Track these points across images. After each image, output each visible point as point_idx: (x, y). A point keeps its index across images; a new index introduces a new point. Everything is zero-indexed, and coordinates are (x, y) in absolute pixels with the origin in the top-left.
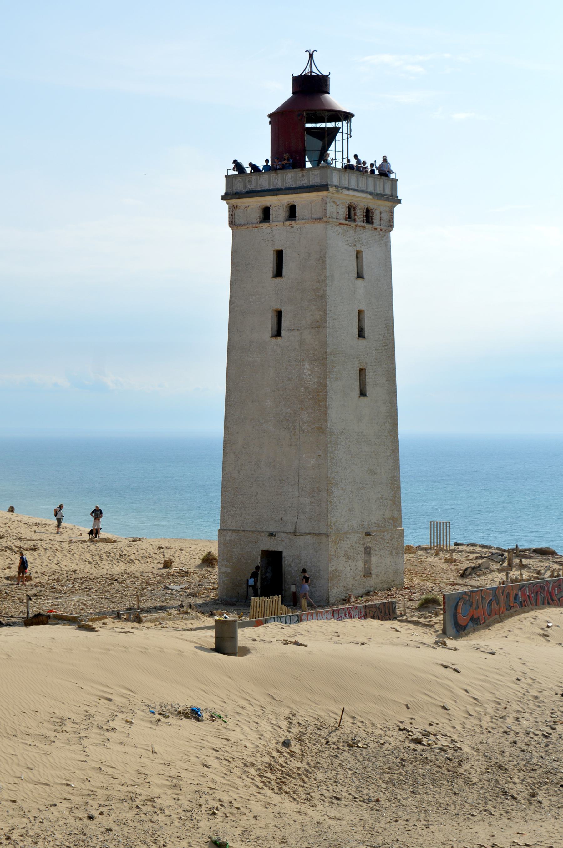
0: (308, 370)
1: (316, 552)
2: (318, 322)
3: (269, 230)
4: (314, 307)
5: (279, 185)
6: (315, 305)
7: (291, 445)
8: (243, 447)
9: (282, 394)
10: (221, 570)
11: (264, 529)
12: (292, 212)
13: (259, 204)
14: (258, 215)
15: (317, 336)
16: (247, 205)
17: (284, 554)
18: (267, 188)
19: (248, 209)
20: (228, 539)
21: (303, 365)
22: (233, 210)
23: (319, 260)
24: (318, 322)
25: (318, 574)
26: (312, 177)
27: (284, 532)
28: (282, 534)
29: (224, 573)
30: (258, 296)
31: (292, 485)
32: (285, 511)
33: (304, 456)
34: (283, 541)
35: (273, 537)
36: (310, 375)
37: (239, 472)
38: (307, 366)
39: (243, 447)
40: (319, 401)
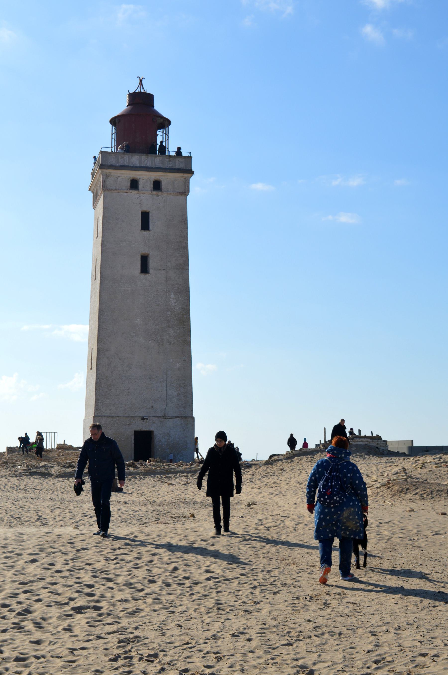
0: (173, 298)
1: (184, 430)
3: (137, 195)
4: (177, 255)
5: (149, 165)
6: (178, 253)
8: (116, 354)
11: (136, 415)
12: (157, 185)
13: (130, 176)
15: (181, 275)
16: (119, 175)
17: (155, 433)
18: (138, 165)
19: (119, 179)
22: (105, 177)
23: (181, 222)
26: (177, 163)
28: (154, 418)
30: (128, 243)
33: (171, 360)
35: (145, 421)
37: (112, 372)
38: (172, 296)
39: (116, 354)
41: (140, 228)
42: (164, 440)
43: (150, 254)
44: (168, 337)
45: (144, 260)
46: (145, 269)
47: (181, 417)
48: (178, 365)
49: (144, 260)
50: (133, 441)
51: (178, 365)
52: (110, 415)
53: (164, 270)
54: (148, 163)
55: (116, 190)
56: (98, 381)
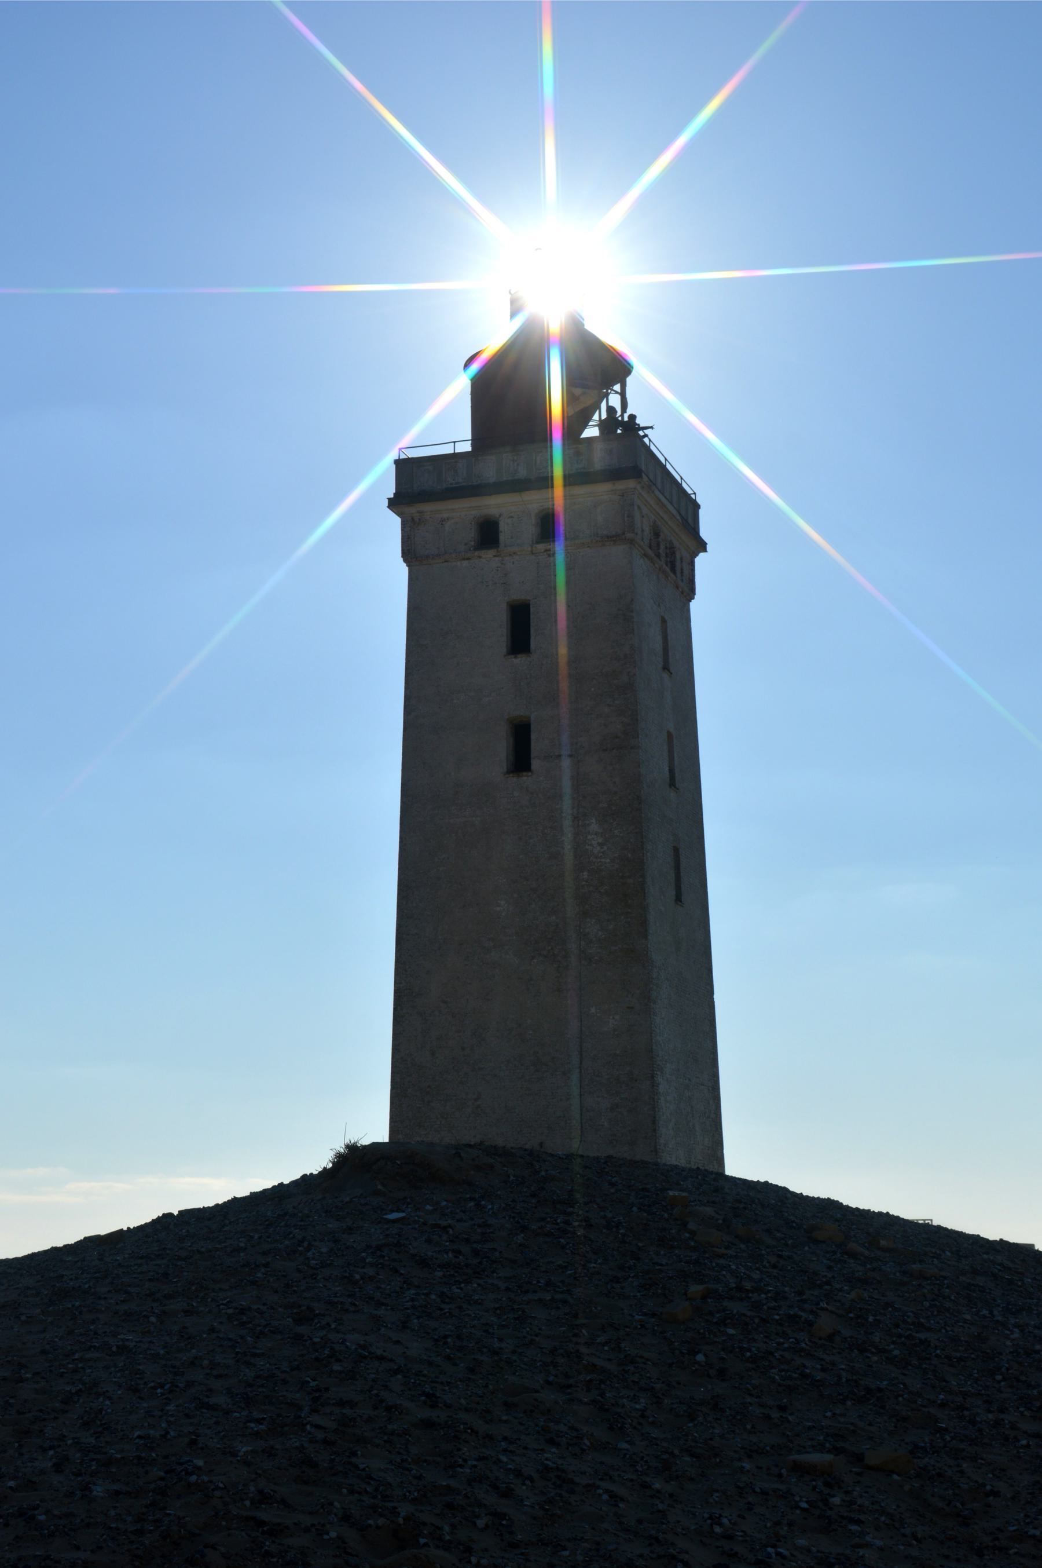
5: (522, 473)
14: (470, 535)
16: (445, 516)
18: (492, 480)
33: (593, 1010)
36: (600, 845)
38: (594, 827)
43: (532, 719)
44: (583, 943)
45: (521, 734)
46: (521, 761)
49: (521, 734)
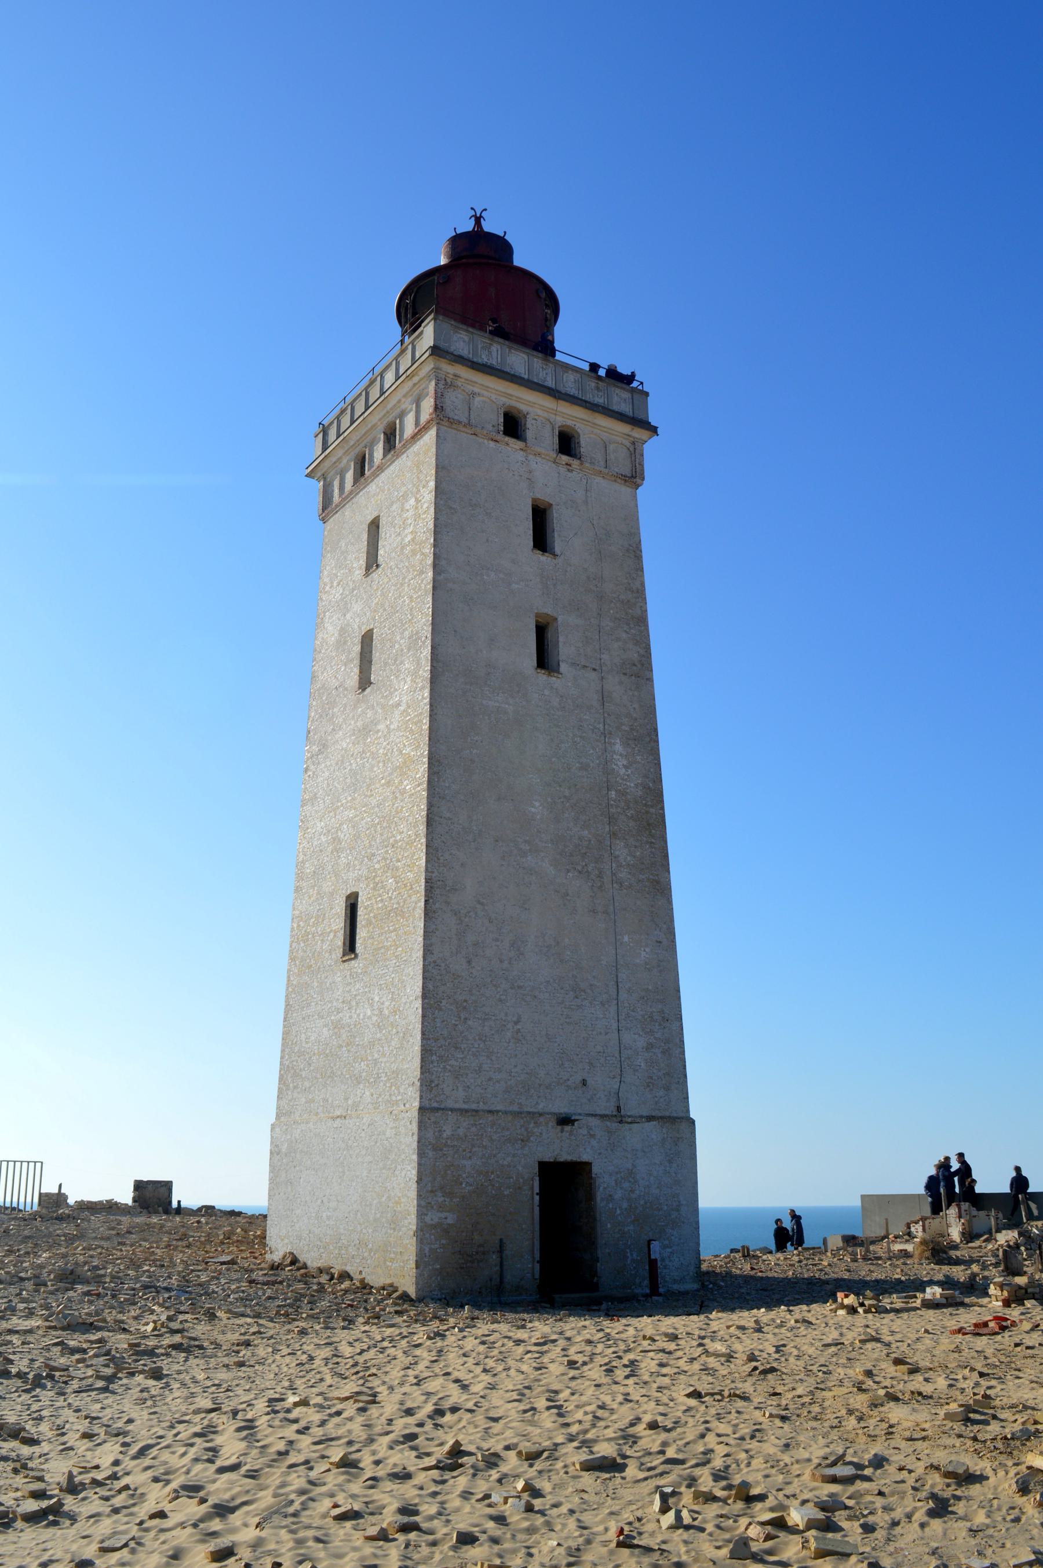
1: (670, 1162)
2: (634, 665)
3: (520, 456)
4: (624, 635)
5: (550, 383)
7: (594, 911)
8: (479, 902)
9: (567, 793)
10: (428, 1219)
11: (540, 1107)
12: (567, 443)
15: (636, 693)
16: (476, 390)
17: (595, 1169)
19: (477, 399)
20: (448, 1132)
21: (610, 743)
24: (634, 665)
25: (674, 1215)
27: (596, 1115)
28: (590, 1119)
29: (434, 1226)
30: (501, 576)
31: (602, 1004)
32: (591, 1064)
33: (626, 939)
34: (592, 1136)
35: (568, 1128)
36: (626, 767)
37: (469, 962)
38: (618, 747)
39: (479, 902)
40: (649, 825)
41: (532, 543)
42: (618, 1195)
43: (560, 619)
47: (662, 1118)
48: (643, 953)
50: (537, 1198)
51: (643, 953)
52: (465, 1106)
53: (594, 670)
54: (549, 379)
55: (469, 424)
56: (431, 987)
